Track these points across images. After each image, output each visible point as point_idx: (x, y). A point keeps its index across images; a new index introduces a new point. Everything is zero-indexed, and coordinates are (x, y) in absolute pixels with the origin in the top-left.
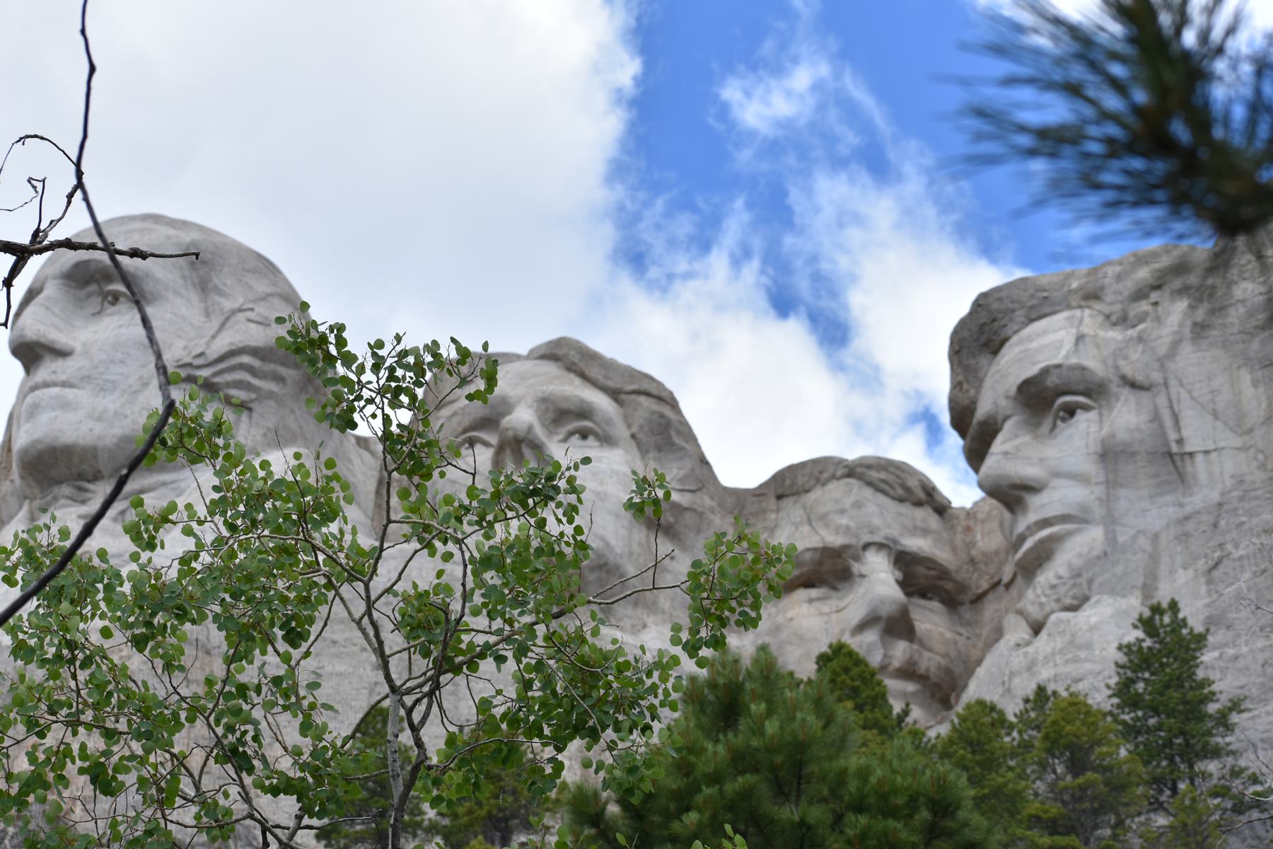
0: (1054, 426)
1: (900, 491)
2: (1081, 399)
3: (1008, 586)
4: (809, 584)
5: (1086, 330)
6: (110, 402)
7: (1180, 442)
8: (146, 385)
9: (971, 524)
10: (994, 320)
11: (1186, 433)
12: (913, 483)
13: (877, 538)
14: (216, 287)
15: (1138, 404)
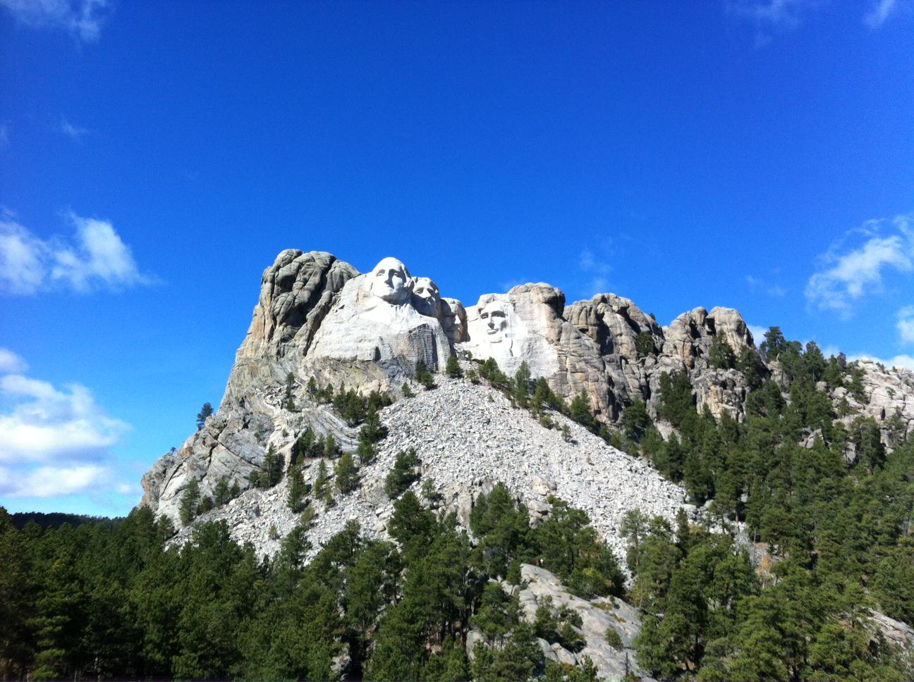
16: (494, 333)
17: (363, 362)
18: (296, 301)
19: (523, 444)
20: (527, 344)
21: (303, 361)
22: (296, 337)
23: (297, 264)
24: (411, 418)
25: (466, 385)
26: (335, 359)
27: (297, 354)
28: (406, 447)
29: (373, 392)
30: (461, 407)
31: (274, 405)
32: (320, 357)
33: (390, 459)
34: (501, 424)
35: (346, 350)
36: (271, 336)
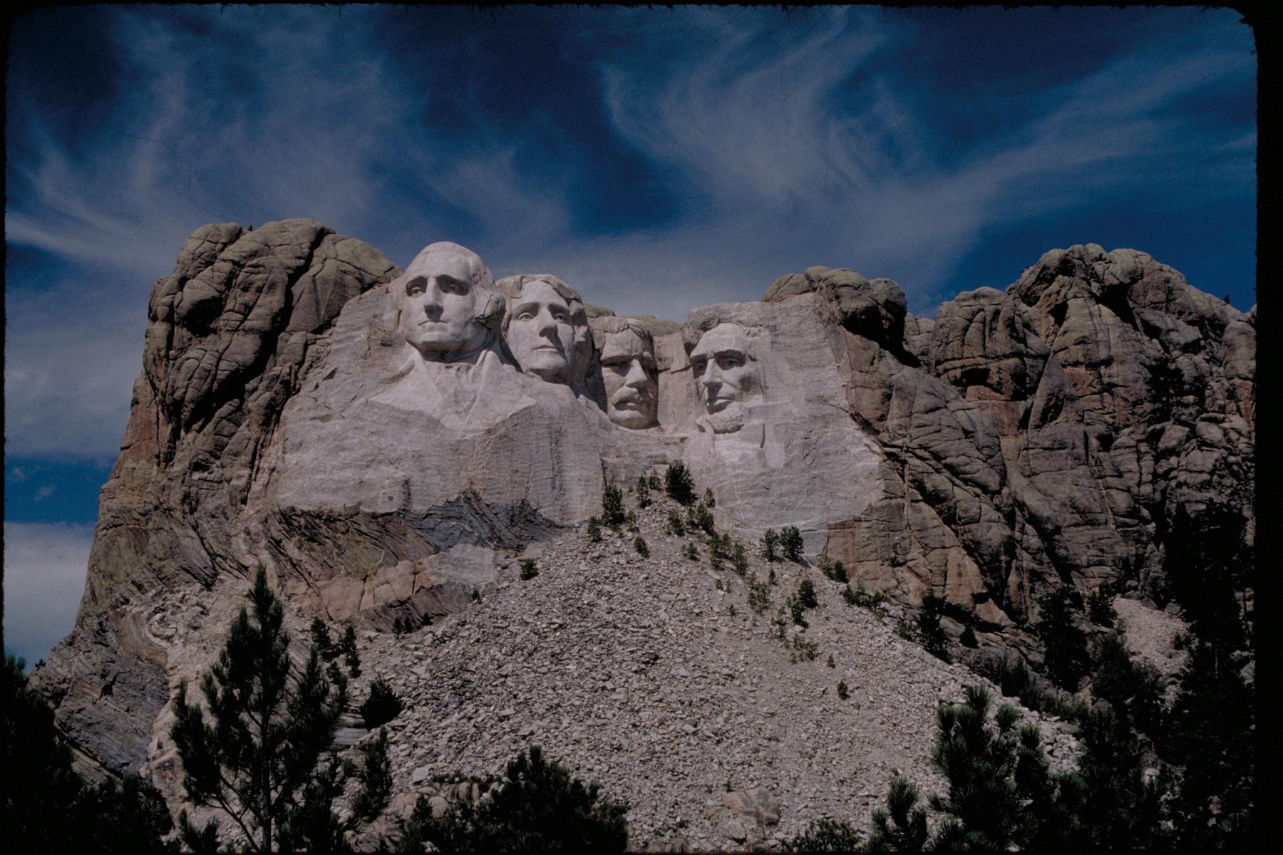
6: (458, 330)
16: (721, 408)
17: (374, 516)
18: (223, 365)
19: (725, 714)
20: (802, 433)
21: (243, 516)
22: (225, 459)
23: (227, 267)
26: (308, 513)
27: (225, 500)
28: (450, 732)
31: (169, 639)
32: (276, 509)
33: (410, 764)
35: (336, 491)
36: (168, 459)
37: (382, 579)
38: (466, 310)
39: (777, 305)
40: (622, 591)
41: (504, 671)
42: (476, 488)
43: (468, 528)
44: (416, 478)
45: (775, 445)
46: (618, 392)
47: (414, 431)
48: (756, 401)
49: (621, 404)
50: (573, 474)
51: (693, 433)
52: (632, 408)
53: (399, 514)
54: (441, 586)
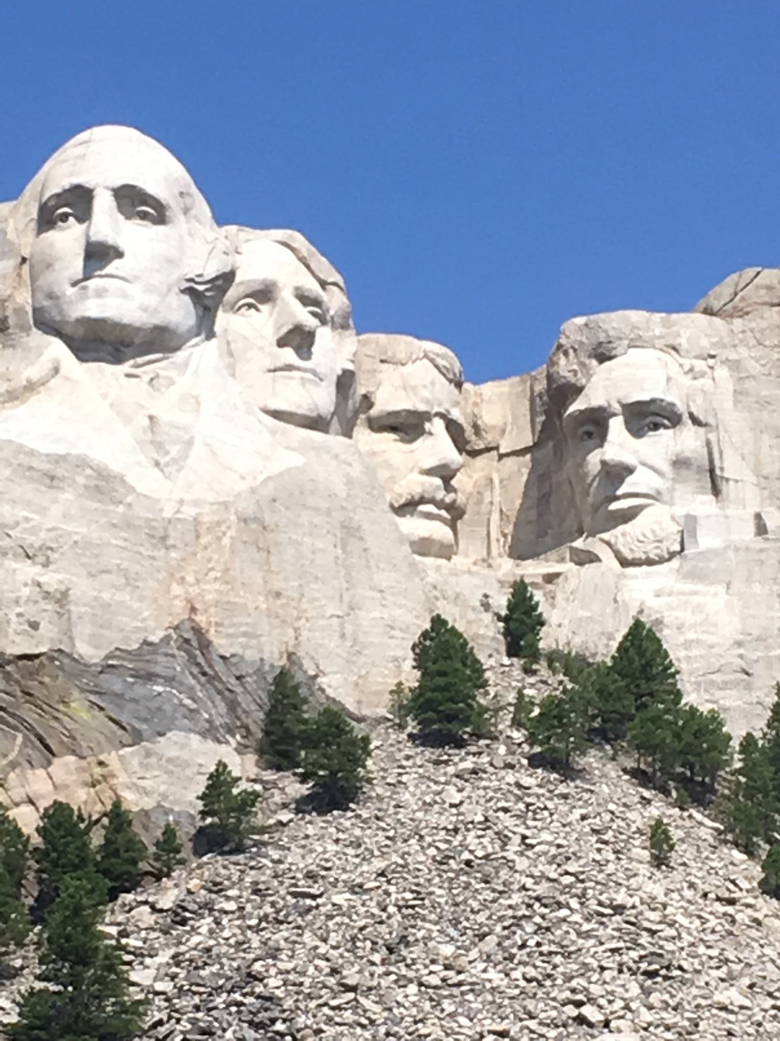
0: (642, 429)
1: (451, 376)
2: (666, 422)
3: (501, 457)
4: (393, 429)
5: (671, 375)
6: (152, 300)
7: (722, 469)
8: (169, 290)
9: (478, 400)
10: (610, 342)
11: (725, 465)
12: (457, 371)
13: (442, 411)
14: (195, 217)
15: (696, 432)
24: (274, 953)
25: (527, 781)
29: (59, 819)
30: (516, 898)
34: (729, 980)
37: (18, 793)
38: (171, 262)
39: (738, 323)
40: (546, 836)
41: (351, 976)
42: (201, 619)
43: (188, 702)
44: (83, 588)
45: (757, 588)
46: (403, 483)
47: (68, 496)
48: (702, 504)
49: (408, 507)
50: (371, 615)
51: (568, 567)
52: (428, 516)
53: (52, 659)
54: (146, 813)
